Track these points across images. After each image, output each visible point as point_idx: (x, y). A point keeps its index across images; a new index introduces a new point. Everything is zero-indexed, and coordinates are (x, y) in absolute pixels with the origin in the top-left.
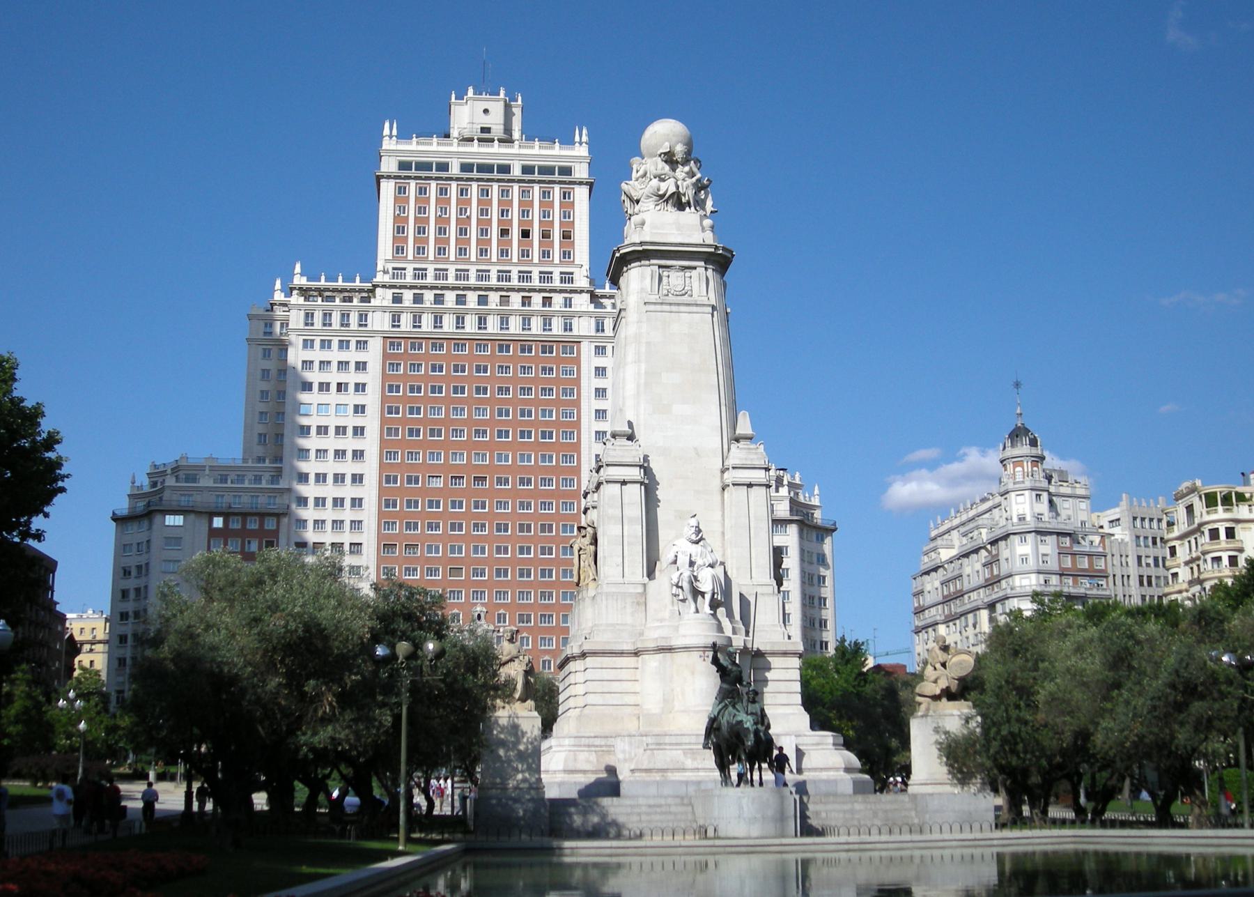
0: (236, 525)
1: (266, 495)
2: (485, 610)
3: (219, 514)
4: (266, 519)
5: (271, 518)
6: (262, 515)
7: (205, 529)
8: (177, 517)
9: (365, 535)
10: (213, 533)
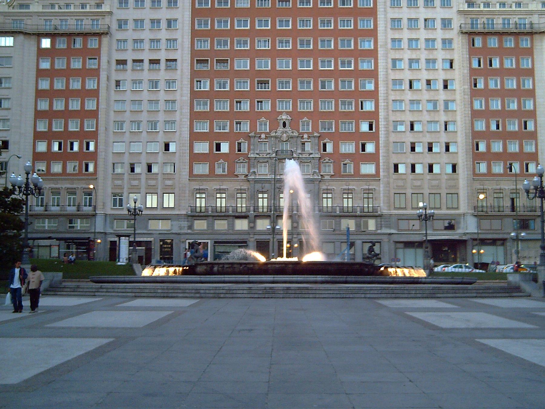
0: (62, 44)
1: (90, 18)
2: (289, 118)
3: (47, 35)
4: (89, 39)
5: (94, 38)
6: (85, 35)
7: (34, 49)
8: (7, 38)
9: (179, 52)
10: (42, 53)
